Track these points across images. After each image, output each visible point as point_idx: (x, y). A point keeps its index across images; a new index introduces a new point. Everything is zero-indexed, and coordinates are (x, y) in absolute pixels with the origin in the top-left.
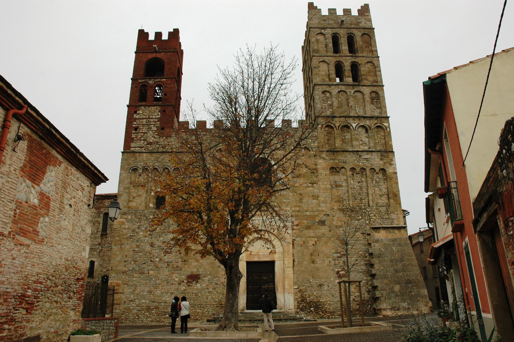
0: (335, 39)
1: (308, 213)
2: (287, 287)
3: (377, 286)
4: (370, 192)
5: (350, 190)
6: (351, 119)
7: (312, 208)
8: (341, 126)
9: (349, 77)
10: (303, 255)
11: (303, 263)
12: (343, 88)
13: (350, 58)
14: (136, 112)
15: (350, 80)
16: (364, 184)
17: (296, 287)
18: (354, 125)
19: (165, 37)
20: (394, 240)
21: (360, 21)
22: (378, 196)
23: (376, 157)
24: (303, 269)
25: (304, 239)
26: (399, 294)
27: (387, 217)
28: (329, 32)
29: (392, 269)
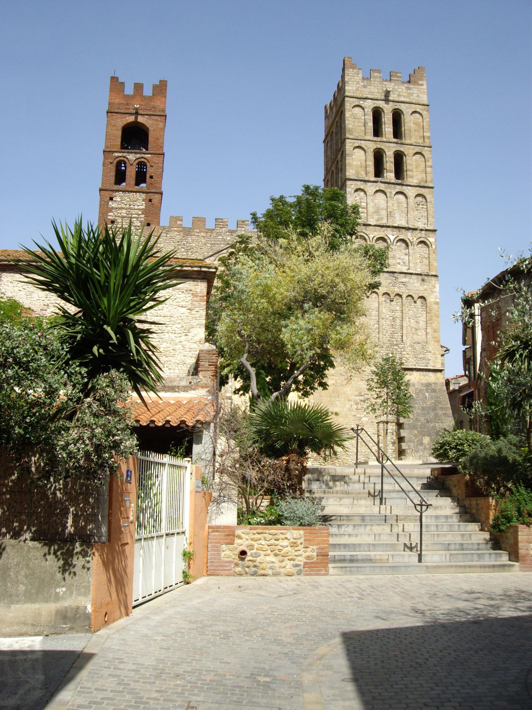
0: (377, 114)
3: (404, 437)
4: (405, 325)
6: (389, 229)
8: (375, 238)
9: (391, 172)
12: (382, 187)
13: (395, 145)
14: (111, 199)
15: (390, 176)
16: (398, 314)
18: (392, 238)
19: (148, 91)
20: (428, 385)
21: (411, 91)
22: (414, 330)
23: (415, 281)
26: (427, 447)
27: (422, 356)
28: (369, 105)
29: (422, 419)
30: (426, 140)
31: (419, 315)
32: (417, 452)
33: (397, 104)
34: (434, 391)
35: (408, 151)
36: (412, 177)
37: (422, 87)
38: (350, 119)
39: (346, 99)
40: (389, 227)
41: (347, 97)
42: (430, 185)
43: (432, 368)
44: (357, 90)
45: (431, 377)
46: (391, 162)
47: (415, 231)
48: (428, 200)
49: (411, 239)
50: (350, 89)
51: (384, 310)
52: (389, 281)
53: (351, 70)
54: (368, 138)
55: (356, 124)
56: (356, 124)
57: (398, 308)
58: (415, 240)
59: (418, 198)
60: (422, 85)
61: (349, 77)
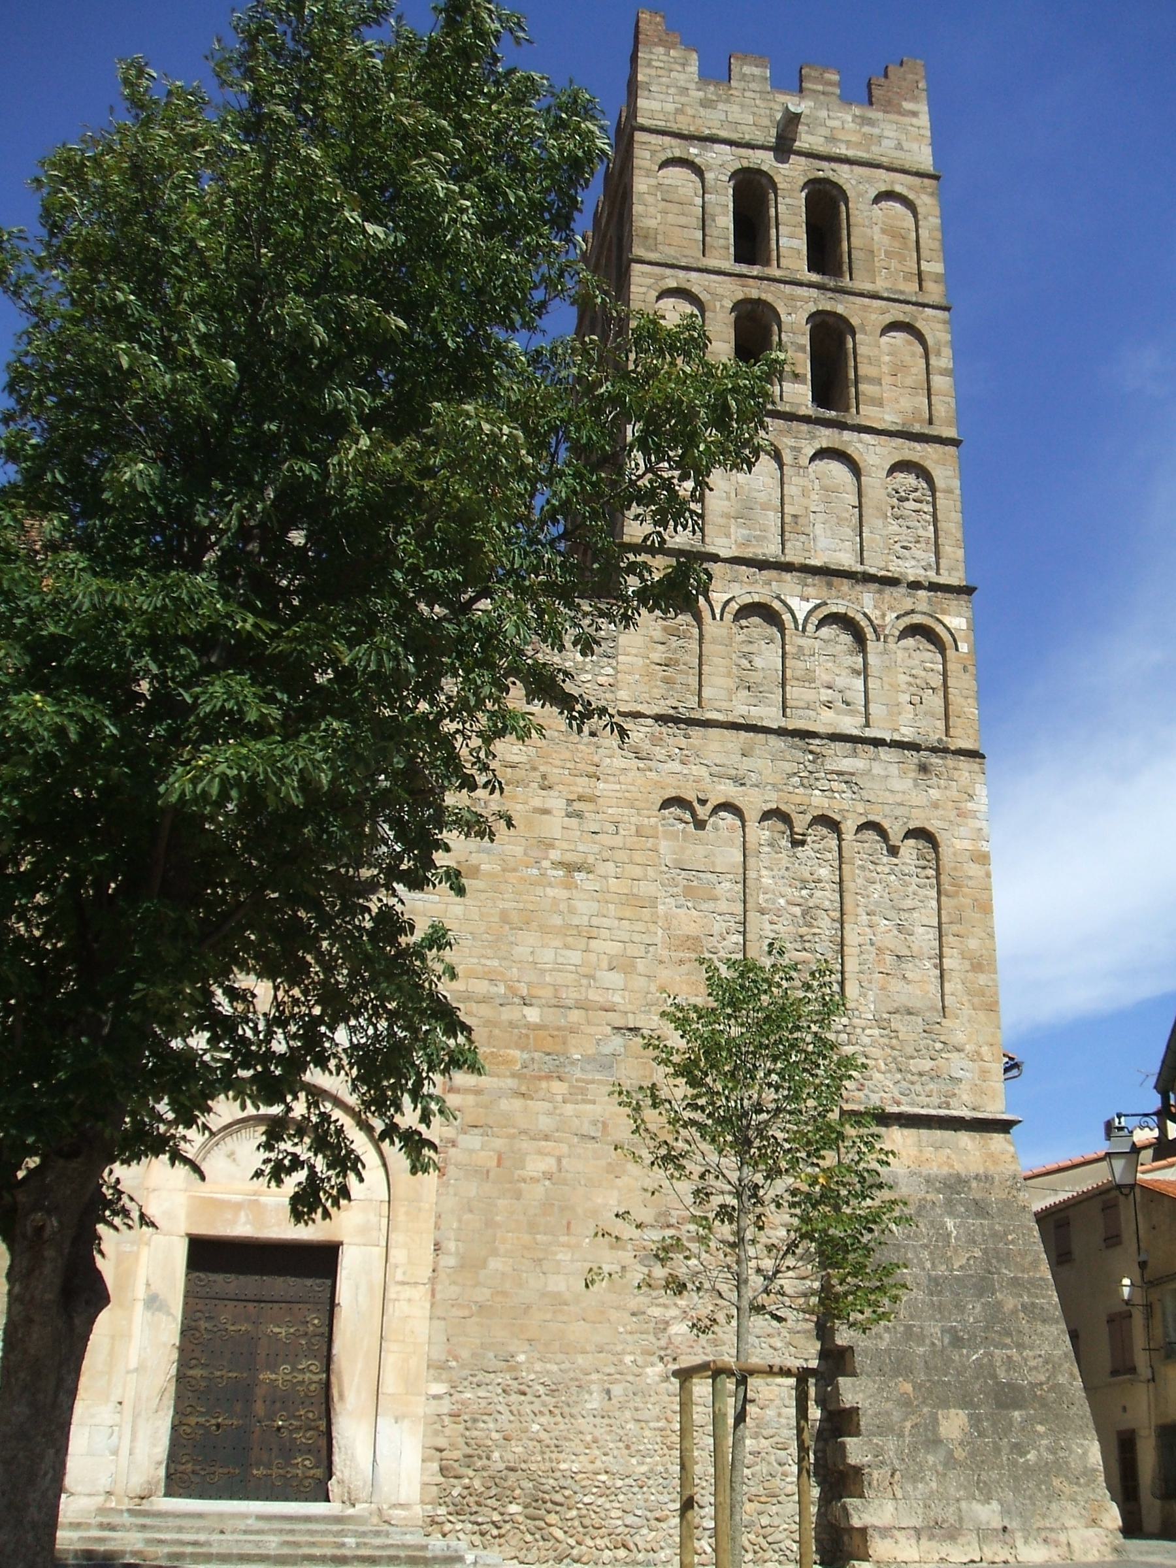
0: (752, 192)
1: (533, 1015)
2: (390, 1384)
3: (855, 1410)
4: (851, 938)
5: (751, 915)
6: (787, 576)
7: (556, 987)
8: (734, 606)
10: (489, 1224)
11: (484, 1264)
13: (814, 292)
16: (827, 896)
17: (439, 1388)
18: (802, 609)
20: (954, 1185)
21: (876, 131)
22: (889, 959)
23: (894, 770)
24: (482, 1295)
25: (499, 1143)
26: (960, 1454)
27: (927, 1065)
28: (721, 162)
29: (934, 1329)
30: (929, 285)
31: (908, 903)
32: (914, 1479)
33: (825, 165)
34: (980, 1209)
35: (867, 317)
36: (879, 403)
37: (914, 121)
38: (650, 199)
39: (639, 136)
40: (788, 567)
41: (643, 129)
42: (950, 432)
43: (967, 1114)
44: (680, 111)
45: (968, 1153)
46: (801, 348)
47: (888, 590)
48: (939, 483)
49: (874, 614)
50: (650, 108)
51: (768, 878)
52: (790, 767)
53: (661, 50)
54: (712, 263)
55: (671, 218)
56: (671, 218)
57: (824, 872)
58: (891, 622)
59: (900, 476)
60: (915, 114)
61: (653, 72)
